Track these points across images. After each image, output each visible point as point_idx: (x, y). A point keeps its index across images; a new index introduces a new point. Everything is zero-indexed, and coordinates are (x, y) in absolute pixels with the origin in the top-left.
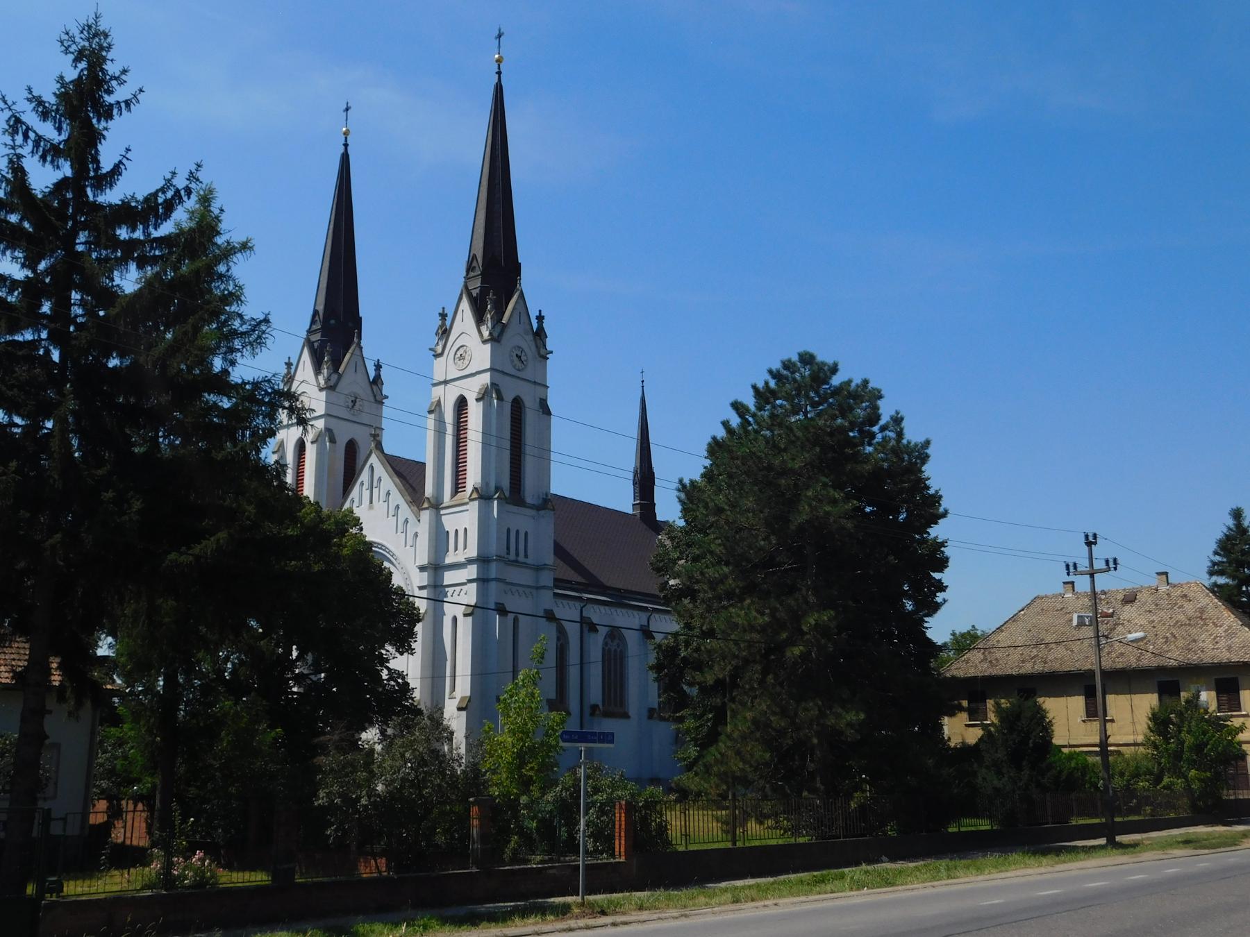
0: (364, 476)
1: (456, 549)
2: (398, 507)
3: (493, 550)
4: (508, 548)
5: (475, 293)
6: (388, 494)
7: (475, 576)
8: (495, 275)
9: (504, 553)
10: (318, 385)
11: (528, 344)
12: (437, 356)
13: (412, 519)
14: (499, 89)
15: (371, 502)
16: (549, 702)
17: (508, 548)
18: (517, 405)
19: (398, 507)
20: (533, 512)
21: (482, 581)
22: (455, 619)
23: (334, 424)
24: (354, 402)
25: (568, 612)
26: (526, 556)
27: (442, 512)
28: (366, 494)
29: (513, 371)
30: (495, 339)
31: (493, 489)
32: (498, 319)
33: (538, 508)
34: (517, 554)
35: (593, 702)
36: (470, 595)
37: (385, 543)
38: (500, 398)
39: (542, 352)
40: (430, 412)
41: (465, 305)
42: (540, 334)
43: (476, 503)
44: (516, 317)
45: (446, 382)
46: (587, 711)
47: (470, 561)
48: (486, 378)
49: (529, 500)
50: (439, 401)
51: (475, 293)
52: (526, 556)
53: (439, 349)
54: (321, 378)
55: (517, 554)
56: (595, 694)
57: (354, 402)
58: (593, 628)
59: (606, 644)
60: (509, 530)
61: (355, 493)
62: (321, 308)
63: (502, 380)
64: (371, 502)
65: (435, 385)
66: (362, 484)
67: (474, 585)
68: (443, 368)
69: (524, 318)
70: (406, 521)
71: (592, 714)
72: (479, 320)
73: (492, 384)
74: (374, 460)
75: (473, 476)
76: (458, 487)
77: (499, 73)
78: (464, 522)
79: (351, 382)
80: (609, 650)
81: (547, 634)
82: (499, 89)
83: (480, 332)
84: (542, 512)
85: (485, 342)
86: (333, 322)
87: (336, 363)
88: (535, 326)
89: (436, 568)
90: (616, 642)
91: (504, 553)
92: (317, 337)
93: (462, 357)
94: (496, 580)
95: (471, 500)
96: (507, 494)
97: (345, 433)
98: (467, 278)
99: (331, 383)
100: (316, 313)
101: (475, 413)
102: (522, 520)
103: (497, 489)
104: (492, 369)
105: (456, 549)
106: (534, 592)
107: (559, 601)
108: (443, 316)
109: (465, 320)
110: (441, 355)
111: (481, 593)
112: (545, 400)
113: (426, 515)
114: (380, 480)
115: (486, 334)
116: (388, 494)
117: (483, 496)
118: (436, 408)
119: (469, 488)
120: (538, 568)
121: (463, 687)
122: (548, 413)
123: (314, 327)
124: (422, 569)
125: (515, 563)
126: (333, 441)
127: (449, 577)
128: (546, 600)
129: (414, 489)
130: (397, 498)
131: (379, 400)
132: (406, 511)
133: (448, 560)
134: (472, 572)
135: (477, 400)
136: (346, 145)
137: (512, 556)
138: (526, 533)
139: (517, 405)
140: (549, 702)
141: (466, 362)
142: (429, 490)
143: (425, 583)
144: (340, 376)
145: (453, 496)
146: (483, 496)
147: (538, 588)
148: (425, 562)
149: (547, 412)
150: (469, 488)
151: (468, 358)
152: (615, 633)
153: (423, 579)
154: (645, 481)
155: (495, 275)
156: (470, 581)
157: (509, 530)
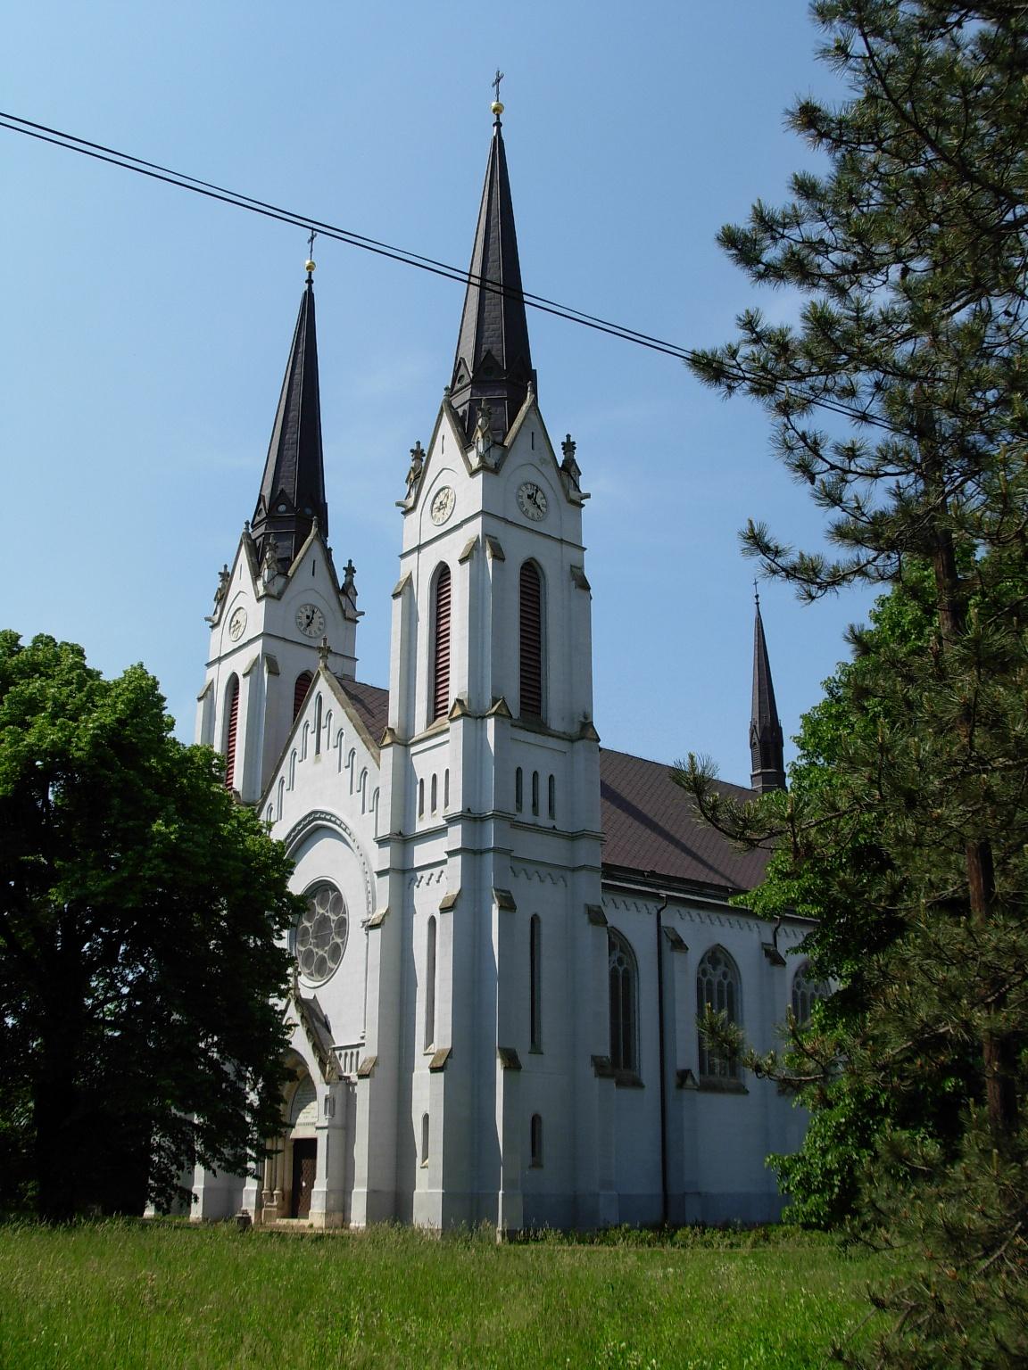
0: (310, 714)
1: (434, 808)
2: (352, 753)
5: (460, 411)
6: (340, 734)
7: (459, 846)
8: (496, 385)
9: (511, 807)
10: (257, 592)
12: (407, 512)
13: (371, 765)
14: (498, 146)
15: (318, 752)
16: (598, 1063)
18: (531, 574)
19: (352, 753)
20: (563, 746)
21: (470, 853)
22: (432, 921)
23: (278, 649)
24: (310, 619)
25: (636, 922)
27: (413, 750)
28: (312, 738)
30: (490, 468)
32: (495, 441)
33: (572, 740)
34: (536, 812)
35: (681, 1065)
36: (450, 881)
38: (498, 556)
39: (574, 495)
40: (395, 596)
41: (447, 428)
42: (569, 470)
43: (460, 723)
45: (419, 548)
46: (672, 1080)
47: (452, 820)
48: (475, 529)
49: (556, 724)
50: (409, 579)
51: (460, 411)
53: (410, 502)
54: (260, 583)
56: (686, 1054)
57: (310, 619)
58: (679, 944)
59: (704, 972)
60: (519, 771)
61: (297, 743)
62: (267, 493)
64: (318, 752)
65: (403, 556)
66: (307, 726)
67: (458, 859)
68: (417, 527)
69: (539, 440)
70: (364, 773)
71: (681, 1085)
72: (466, 443)
73: (485, 535)
74: (322, 686)
75: (458, 685)
76: (436, 710)
78: (442, 760)
79: (307, 585)
80: (709, 982)
81: (592, 943)
82: (498, 146)
84: (579, 745)
85: (473, 474)
86: (282, 508)
87: (283, 565)
89: (402, 839)
90: (721, 968)
91: (511, 807)
92: (262, 529)
93: (443, 506)
94: (494, 850)
95: (452, 720)
96: (516, 713)
97: (294, 663)
98: (451, 392)
99: (274, 591)
100: (261, 498)
101: (460, 581)
102: (539, 756)
104: (482, 512)
105: (434, 808)
106: (569, 874)
107: (619, 899)
108: (418, 454)
110: (413, 508)
111: (472, 877)
112: (581, 568)
113: (388, 755)
114: (329, 715)
115: (475, 461)
116: (340, 734)
117: (472, 714)
118: (405, 590)
119: (451, 703)
120: (574, 837)
121: (444, 1038)
122: (588, 588)
123: (258, 519)
124: (382, 842)
126: (274, 671)
127: (423, 854)
128: (590, 889)
129: (369, 711)
130: (353, 739)
131: (350, 618)
132: (363, 756)
133: (421, 826)
134: (455, 837)
135: (462, 561)
136: (310, 281)
137: (526, 816)
138: (551, 778)
139: (531, 574)
140: (598, 1063)
141: (448, 511)
142: (394, 718)
143: (388, 866)
144: (288, 580)
145: (429, 723)
146: (472, 714)
147: (574, 870)
148: (385, 831)
149: (584, 585)
150: (451, 703)
151: (450, 504)
152: (717, 957)
153: (382, 858)
154: (767, 741)
155: (496, 385)
156: (451, 854)
157: (519, 771)
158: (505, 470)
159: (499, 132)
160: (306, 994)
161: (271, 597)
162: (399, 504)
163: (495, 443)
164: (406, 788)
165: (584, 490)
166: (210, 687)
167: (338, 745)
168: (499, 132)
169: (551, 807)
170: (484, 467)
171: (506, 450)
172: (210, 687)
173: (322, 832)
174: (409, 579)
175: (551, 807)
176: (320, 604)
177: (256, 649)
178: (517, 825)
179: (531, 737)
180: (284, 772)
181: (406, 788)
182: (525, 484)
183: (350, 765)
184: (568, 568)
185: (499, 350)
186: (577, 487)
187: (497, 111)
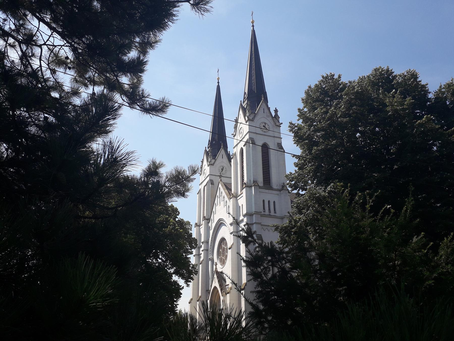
3: (254, 210)
4: (264, 209)
11: (270, 123)
14: (254, 32)
17: (264, 209)
23: (213, 178)
24: (222, 169)
26: (275, 212)
27: (238, 198)
28: (219, 199)
29: (262, 133)
31: (252, 182)
33: (280, 191)
34: (270, 212)
37: (224, 218)
39: (277, 124)
42: (276, 117)
44: (262, 110)
48: (247, 137)
49: (275, 187)
50: (235, 153)
52: (275, 212)
55: (270, 212)
57: (222, 169)
60: (264, 201)
61: (216, 202)
63: (254, 136)
73: (250, 138)
77: (253, 26)
82: (254, 32)
83: (245, 119)
84: (282, 192)
86: (214, 142)
88: (273, 114)
94: (255, 223)
96: (261, 184)
99: (212, 163)
100: (209, 140)
102: (269, 196)
103: (254, 182)
104: (249, 132)
109: (242, 119)
115: (247, 119)
120: (282, 218)
124: (231, 224)
125: (270, 216)
135: (244, 146)
136: (218, 83)
138: (274, 202)
144: (216, 160)
149: (282, 148)
157: (264, 201)
158: (255, 120)
159: (253, 28)
160: (219, 270)
161: (210, 165)
162: (232, 134)
163: (252, 113)
164: (237, 208)
165: (280, 122)
166: (200, 190)
167: (224, 200)
168: (253, 28)
169: (275, 210)
170: (249, 120)
171: (255, 115)
172: (200, 190)
173: (222, 224)
174: (235, 153)
175: (275, 210)
176: (225, 165)
177: (208, 179)
178: (263, 216)
179: (267, 191)
180: (214, 210)
181: (237, 208)
182: (262, 123)
183: (226, 205)
184: (276, 144)
185: (254, 87)
186: (279, 122)
187: (253, 22)
